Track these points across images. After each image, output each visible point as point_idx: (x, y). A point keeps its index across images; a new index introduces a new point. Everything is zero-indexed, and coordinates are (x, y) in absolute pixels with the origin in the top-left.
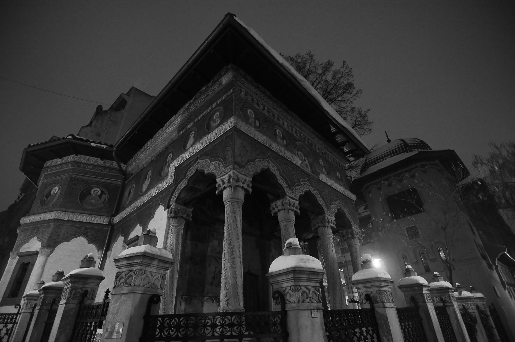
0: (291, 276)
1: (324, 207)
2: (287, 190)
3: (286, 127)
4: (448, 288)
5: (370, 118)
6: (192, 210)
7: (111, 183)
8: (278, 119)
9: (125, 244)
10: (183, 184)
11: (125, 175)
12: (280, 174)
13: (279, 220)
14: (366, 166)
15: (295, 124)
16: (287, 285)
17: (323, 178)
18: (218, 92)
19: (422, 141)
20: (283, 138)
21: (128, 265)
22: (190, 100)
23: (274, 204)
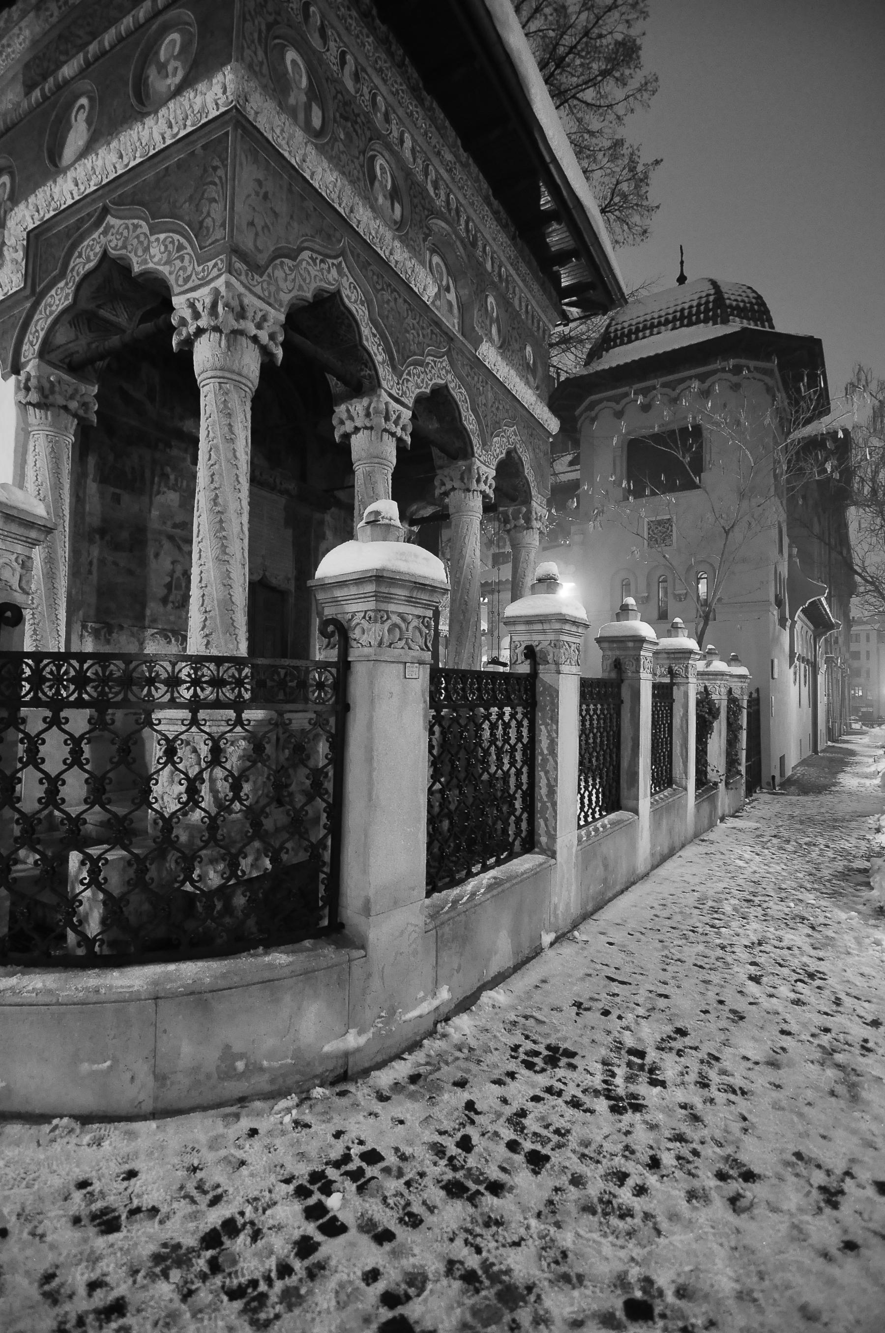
0: (370, 588)
1: (476, 441)
2: (384, 372)
3: (408, 154)
4: (691, 652)
5: (654, 193)
6: (95, 389)
8: (387, 120)
10: (59, 298)
12: (372, 320)
13: (354, 456)
14: (607, 342)
16: (355, 607)
17: (489, 353)
23: (343, 407)
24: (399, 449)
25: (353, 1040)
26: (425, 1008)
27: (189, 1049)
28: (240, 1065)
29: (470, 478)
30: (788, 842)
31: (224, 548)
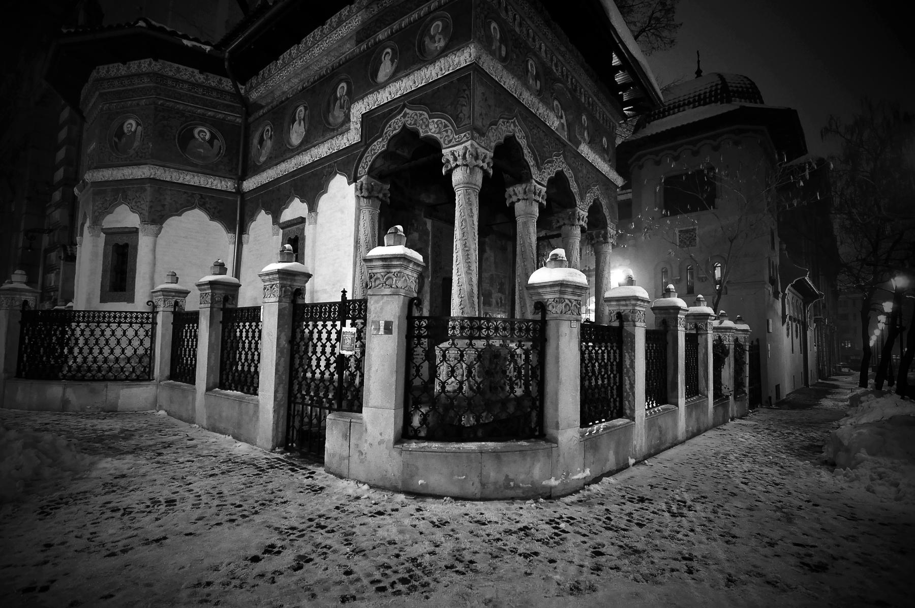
0: (557, 289)
1: (577, 198)
2: (534, 170)
3: (543, 55)
4: (709, 315)
7: (224, 119)
8: (534, 40)
9: (276, 226)
10: (379, 146)
11: (248, 108)
12: (528, 145)
13: (517, 214)
15: (558, 49)
16: (549, 296)
17: (584, 149)
19: (752, 83)
20: (537, 77)
21: (384, 267)
23: (511, 189)
25: (553, 482)
26: (580, 476)
27: (493, 474)
28: (512, 484)
29: (574, 219)
30: (775, 432)
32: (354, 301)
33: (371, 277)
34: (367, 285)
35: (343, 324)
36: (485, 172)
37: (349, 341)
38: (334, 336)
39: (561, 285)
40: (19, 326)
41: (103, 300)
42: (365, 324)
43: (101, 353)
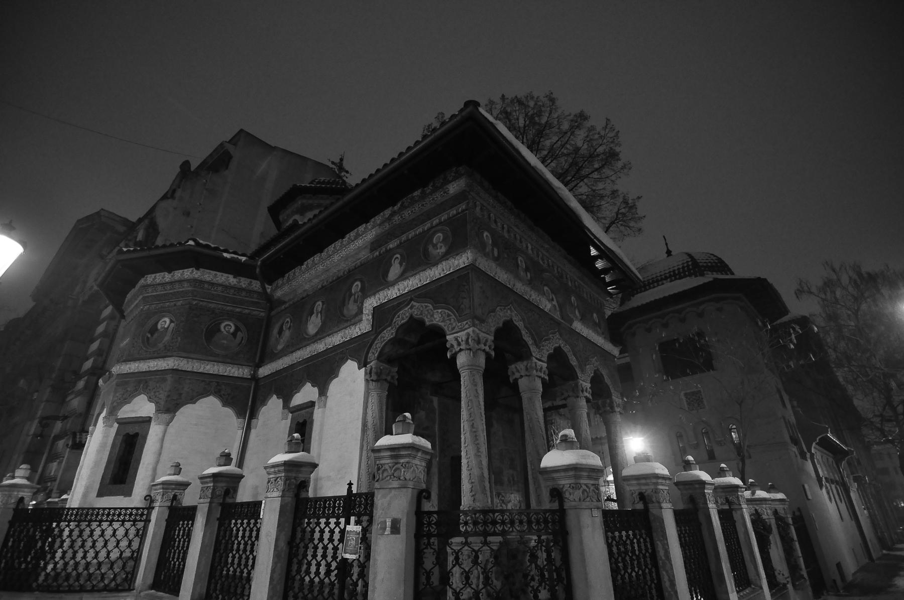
0: (571, 473)
1: (578, 370)
2: (533, 349)
3: (530, 252)
5: (641, 210)
6: (396, 369)
7: (249, 314)
8: (521, 242)
9: (286, 411)
10: (388, 334)
11: (271, 303)
12: (525, 327)
16: (565, 482)
17: (578, 326)
18: (442, 203)
19: (719, 259)
20: (527, 270)
21: (392, 457)
22: (394, 205)
23: (513, 366)
24: (543, 383)
31: (478, 449)
32: (359, 495)
33: (379, 469)
34: (374, 477)
35: (348, 522)
36: (488, 355)
37: (353, 542)
38: (337, 536)
39: (574, 469)
40: (7, 526)
41: (100, 494)
42: (370, 522)
43: (84, 557)
